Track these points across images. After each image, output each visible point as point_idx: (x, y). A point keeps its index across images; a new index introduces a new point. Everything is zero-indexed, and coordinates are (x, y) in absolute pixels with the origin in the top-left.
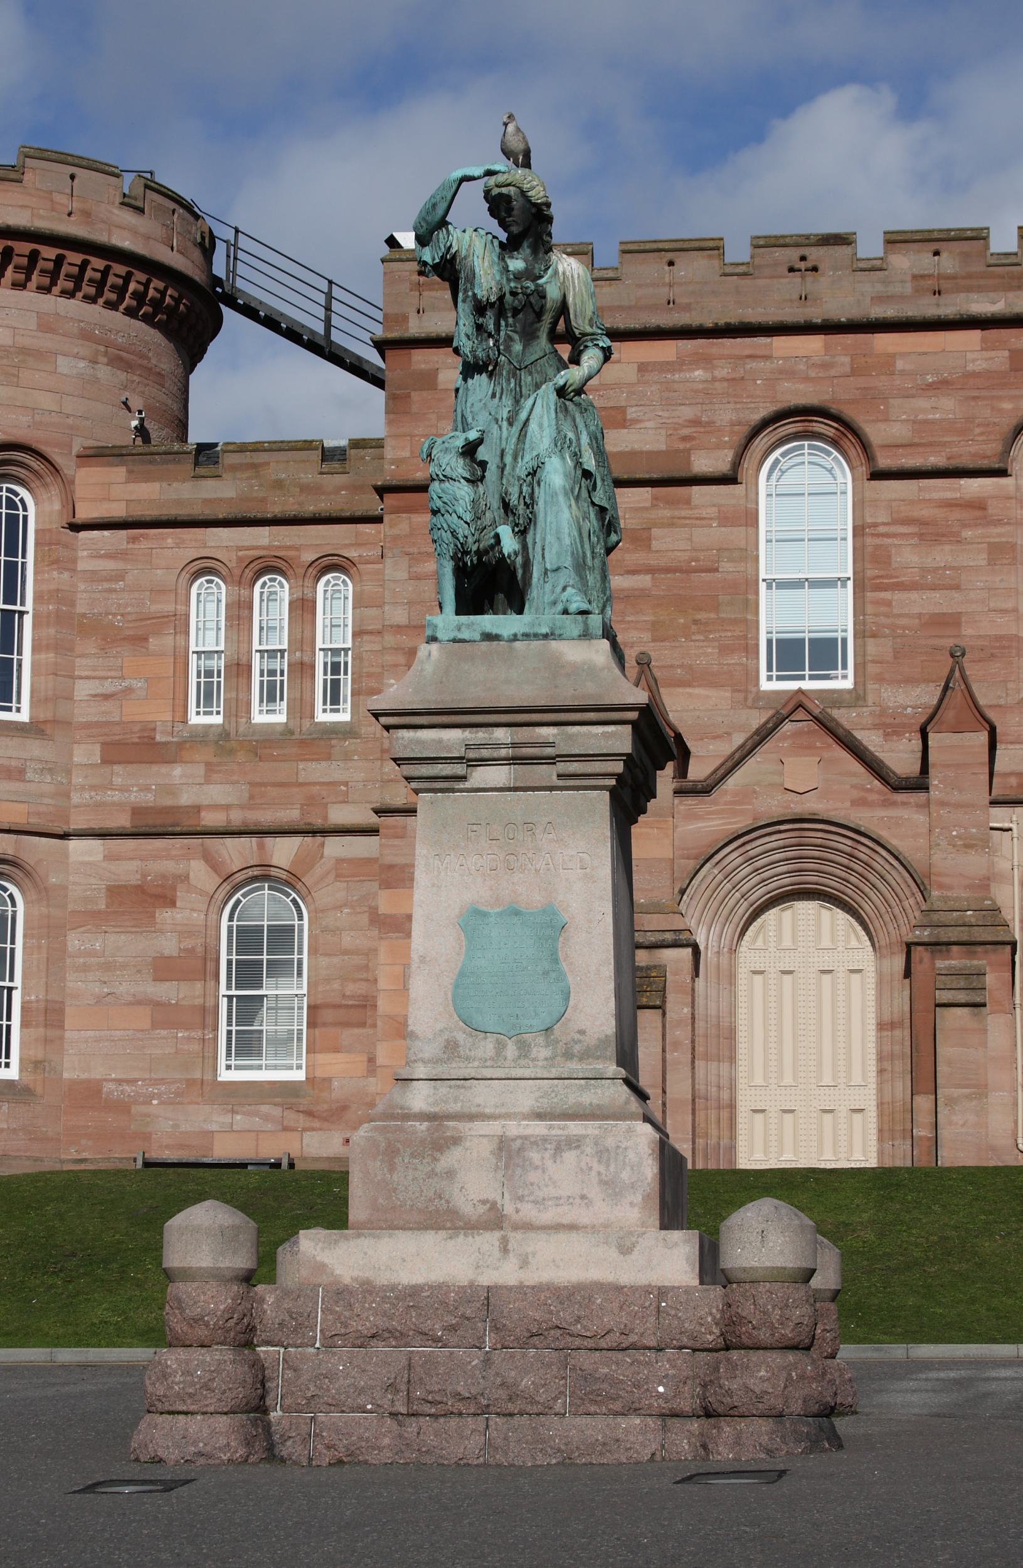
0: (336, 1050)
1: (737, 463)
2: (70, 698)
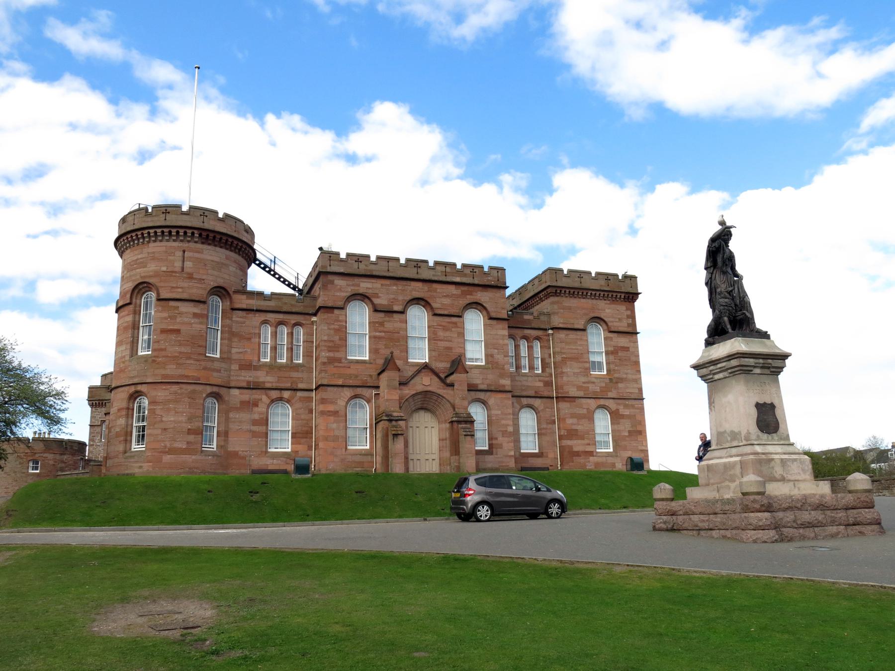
0: (300, 444)
1: (404, 309)
2: (231, 352)
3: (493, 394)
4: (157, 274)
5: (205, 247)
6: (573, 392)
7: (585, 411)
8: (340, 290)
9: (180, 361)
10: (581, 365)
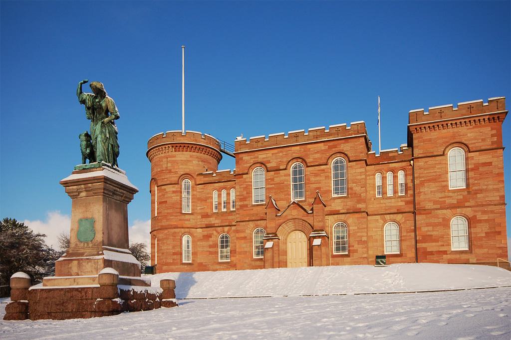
3: (351, 215)
4: (157, 174)
5: (177, 153)
6: (429, 205)
7: (441, 220)
8: (246, 163)
9: (168, 218)
10: (437, 184)
